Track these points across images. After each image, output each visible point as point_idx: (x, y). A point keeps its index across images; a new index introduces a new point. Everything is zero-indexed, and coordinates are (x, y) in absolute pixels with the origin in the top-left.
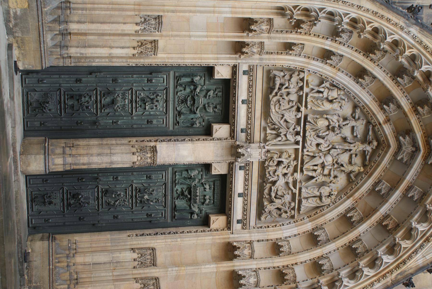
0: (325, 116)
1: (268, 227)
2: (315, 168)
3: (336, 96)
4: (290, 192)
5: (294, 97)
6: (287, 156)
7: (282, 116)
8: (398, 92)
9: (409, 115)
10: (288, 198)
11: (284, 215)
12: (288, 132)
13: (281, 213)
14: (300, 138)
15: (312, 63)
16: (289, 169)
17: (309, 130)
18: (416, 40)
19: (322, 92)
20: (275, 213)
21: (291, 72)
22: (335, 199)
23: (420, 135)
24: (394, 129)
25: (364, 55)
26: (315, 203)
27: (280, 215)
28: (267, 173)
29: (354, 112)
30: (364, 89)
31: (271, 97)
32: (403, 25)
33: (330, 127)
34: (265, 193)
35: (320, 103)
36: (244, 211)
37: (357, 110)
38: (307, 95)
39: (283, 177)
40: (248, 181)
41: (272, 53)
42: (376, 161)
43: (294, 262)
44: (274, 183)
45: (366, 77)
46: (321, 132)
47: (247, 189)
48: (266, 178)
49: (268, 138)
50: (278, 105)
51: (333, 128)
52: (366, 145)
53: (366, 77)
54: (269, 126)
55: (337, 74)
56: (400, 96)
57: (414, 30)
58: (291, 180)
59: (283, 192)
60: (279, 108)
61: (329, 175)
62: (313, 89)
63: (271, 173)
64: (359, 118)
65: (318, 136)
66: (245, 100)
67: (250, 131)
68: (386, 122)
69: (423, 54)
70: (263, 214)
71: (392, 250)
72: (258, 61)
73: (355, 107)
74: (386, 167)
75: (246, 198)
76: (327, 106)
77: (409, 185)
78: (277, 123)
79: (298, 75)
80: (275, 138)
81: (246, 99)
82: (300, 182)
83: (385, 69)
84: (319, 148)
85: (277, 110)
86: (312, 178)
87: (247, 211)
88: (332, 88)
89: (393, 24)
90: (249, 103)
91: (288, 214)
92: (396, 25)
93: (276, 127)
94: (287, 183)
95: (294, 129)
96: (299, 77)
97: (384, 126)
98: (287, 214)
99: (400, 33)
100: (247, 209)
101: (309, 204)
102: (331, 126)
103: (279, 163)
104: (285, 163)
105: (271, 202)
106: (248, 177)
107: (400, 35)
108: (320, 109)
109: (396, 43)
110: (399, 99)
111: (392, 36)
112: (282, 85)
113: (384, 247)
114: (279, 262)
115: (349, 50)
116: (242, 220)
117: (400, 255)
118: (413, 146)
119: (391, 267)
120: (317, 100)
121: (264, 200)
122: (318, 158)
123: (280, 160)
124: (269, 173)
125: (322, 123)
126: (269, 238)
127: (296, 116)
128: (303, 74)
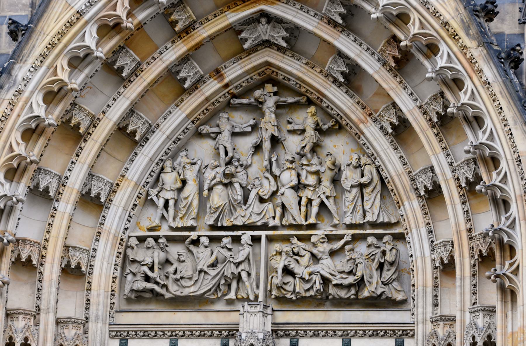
0: (206, 193)
1: (413, 285)
2: (304, 201)
3: (175, 174)
4: (347, 247)
5: (175, 250)
6: (278, 257)
7: (203, 274)
8: (153, 69)
9: (193, 43)
10: (362, 248)
11: (389, 257)
12: (231, 260)
13: (387, 262)
14: (246, 236)
15: (108, 226)
16: (303, 253)
17: (232, 220)
18: (39, 64)
19: (167, 202)
20: (387, 274)
21: (127, 261)
22: (369, 157)
23: (233, 14)
24: (233, 59)
25: (85, 141)
26: (373, 195)
27: (392, 264)
28: (308, 294)
29: (208, 135)
30: (158, 125)
31: (168, 296)
32: (12, 91)
33: (227, 181)
34: (346, 297)
35: (185, 202)
36: (377, 334)
37: (204, 132)
38: (172, 229)
39: (321, 262)
40: (318, 330)
41: (88, 300)
42: (297, 83)
43: (465, 236)
44: (325, 281)
45: (130, 129)
46: (236, 198)
47: (334, 331)
48: (315, 295)
49: (245, 296)
50: (184, 283)
51: (225, 175)
52: (265, 107)
53: (130, 129)
54: (224, 295)
55: (129, 178)
56: (160, 63)
57: (20, 71)
58: (327, 247)
59: (348, 260)
60: (190, 279)
61: (317, 173)
62: (163, 217)
63: (308, 286)
64: (218, 126)
65: (246, 199)
66: (170, 342)
67: (225, 330)
68: (222, 75)
69: (66, 46)
70: (387, 298)
71: (432, 49)
72: (100, 325)
73: (199, 135)
74: (306, 64)
75: (352, 333)
76: (191, 189)
77: (326, 21)
78: (214, 282)
79: (133, 248)
80: (243, 282)
81: (168, 341)
82: (335, 226)
83: (112, 99)
84: (266, 197)
85: (192, 282)
86: (322, 205)
87: (376, 330)
88: (160, 183)
89: (11, 110)
90: (176, 335)
91: (388, 247)
92: (13, 104)
93: (223, 282)
94: (333, 253)
95: (230, 250)
96: (135, 247)
97: (226, 80)
98: (388, 253)
99: (26, 94)
100: (374, 331)
101: (374, 207)
102: (223, 181)
103: (287, 271)
104: (286, 263)
105: (360, 283)
106: (310, 330)
107: (32, 93)
108: (196, 203)
109: (51, 96)
110: (164, 66)
111: (35, 106)
112: (147, 279)
113: (426, 63)
114: (464, 265)
115: (76, 168)
116: (396, 339)
117: (435, 34)
118: (259, 22)
119: (455, 49)
120: (180, 209)
121: (360, 297)
122: (284, 199)
123: (280, 271)
124: (308, 290)
125: (219, 197)
126: (430, 283)
127: (206, 247)
128: (131, 239)
